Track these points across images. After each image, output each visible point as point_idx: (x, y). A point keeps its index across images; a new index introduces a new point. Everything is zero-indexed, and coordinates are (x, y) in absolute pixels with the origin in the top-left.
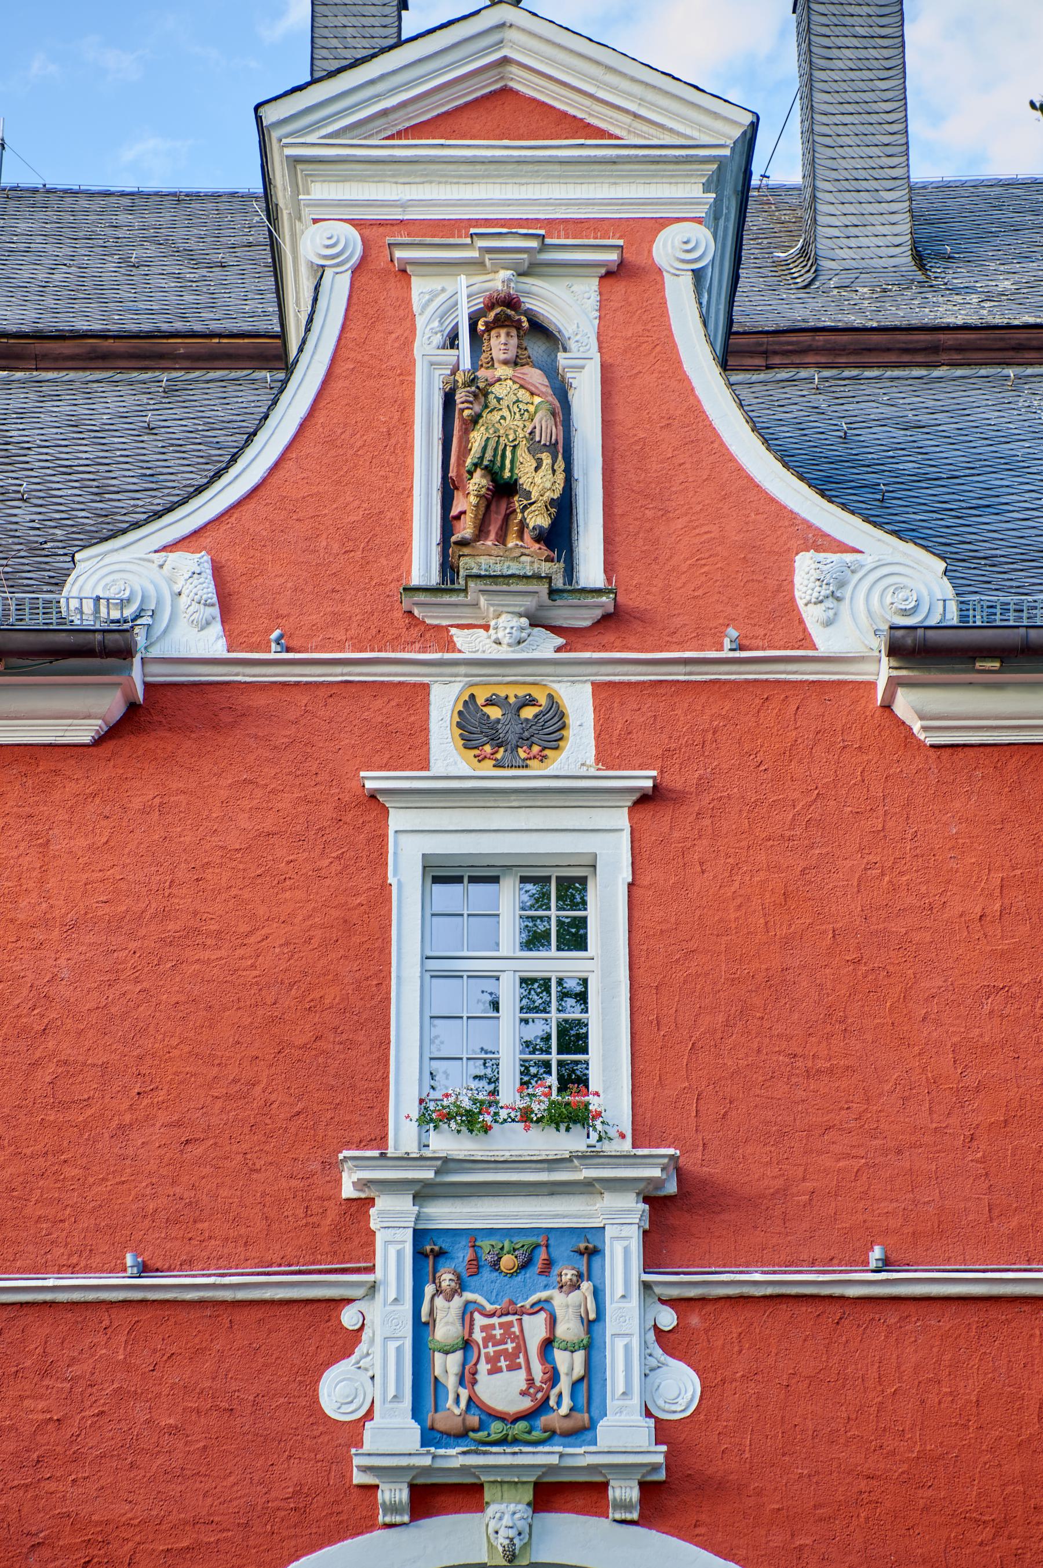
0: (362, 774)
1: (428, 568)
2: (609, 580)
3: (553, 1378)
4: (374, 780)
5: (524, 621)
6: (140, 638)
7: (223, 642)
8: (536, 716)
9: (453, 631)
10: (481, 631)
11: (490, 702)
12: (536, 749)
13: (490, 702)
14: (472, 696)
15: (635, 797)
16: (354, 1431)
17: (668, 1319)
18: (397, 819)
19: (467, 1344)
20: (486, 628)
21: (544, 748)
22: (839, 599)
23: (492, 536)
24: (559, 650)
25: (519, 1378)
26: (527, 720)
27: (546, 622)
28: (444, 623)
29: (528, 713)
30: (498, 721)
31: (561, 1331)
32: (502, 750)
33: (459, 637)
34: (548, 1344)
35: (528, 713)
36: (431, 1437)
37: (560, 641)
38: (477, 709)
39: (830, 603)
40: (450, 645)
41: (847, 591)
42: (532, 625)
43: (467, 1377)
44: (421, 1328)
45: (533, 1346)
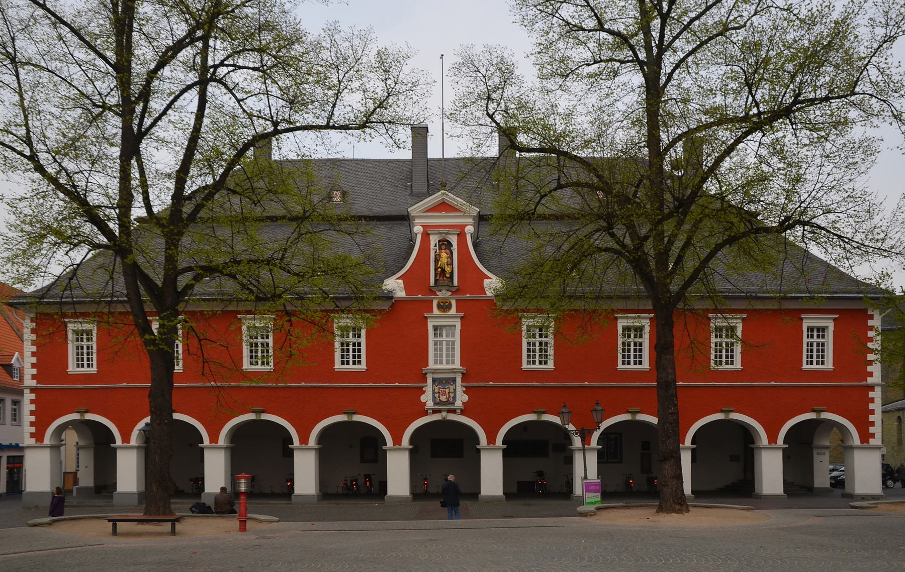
3: (450, 397)
4: (426, 315)
16: (425, 403)
17: (464, 389)
18: (429, 320)
19: (439, 392)
24: (451, 295)
25: (445, 397)
29: (447, 304)
31: (451, 391)
33: (438, 293)
34: (449, 393)
35: (447, 304)
36: (435, 404)
43: (439, 397)
44: (433, 390)
45: (447, 393)
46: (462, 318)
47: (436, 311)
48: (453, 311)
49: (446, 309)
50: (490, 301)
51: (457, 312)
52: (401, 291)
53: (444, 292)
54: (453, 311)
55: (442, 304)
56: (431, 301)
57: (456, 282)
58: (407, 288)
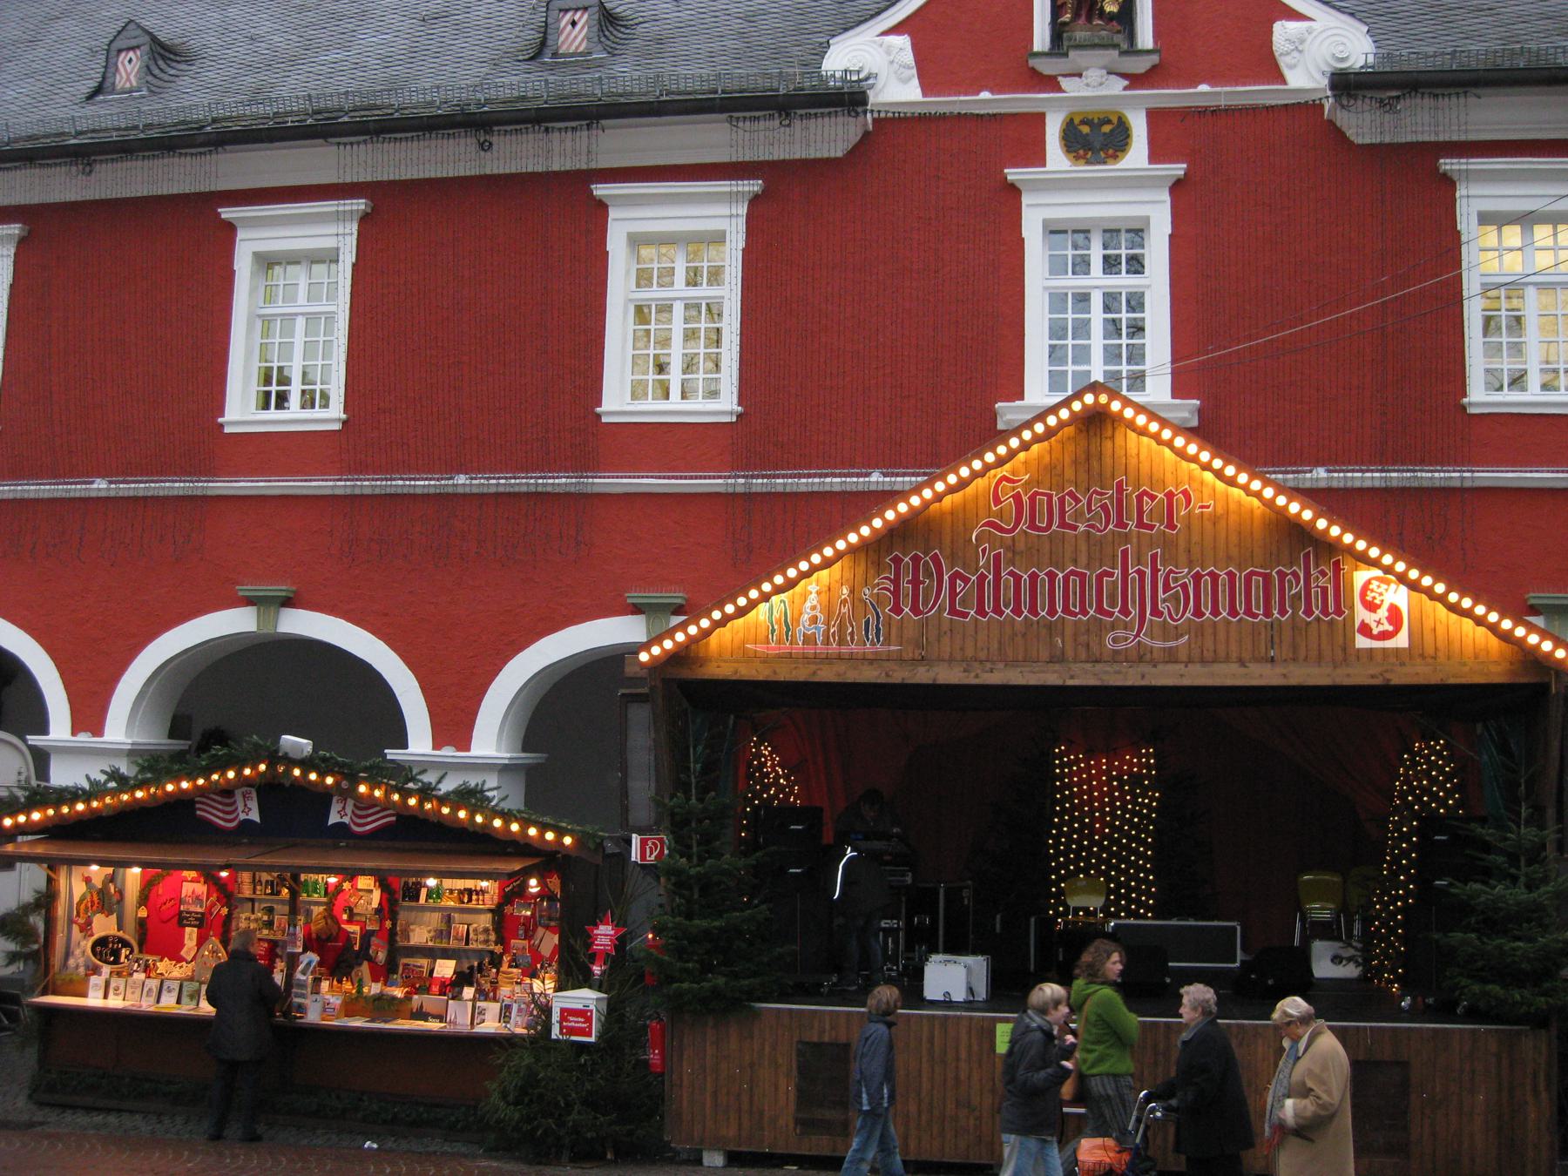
0: (1006, 171)
1: (1043, 40)
2: (1155, 42)
5: (1104, 72)
6: (871, 93)
7: (919, 90)
8: (1111, 131)
9: (1060, 79)
10: (1077, 79)
11: (1083, 122)
12: (1111, 151)
13: (1083, 122)
14: (1072, 120)
15: (1175, 179)
20: (1080, 75)
21: (1116, 151)
22: (1300, 52)
23: (1083, 18)
24: (1125, 88)
26: (1105, 134)
27: (1118, 71)
28: (1054, 73)
29: (1106, 129)
30: (1087, 135)
32: (1090, 153)
35: (1106, 129)
37: (1126, 83)
38: (1075, 128)
39: (1295, 54)
40: (1059, 89)
41: (1305, 46)
42: (1109, 73)
46: (1177, 187)
47: (1056, 157)
48: (1137, 154)
49: (1104, 147)
50: (1307, 109)
51: (1154, 156)
52: (906, 81)
53: (1093, 75)
54: (1137, 154)
55: (1085, 129)
56: (1039, 119)
57: (1145, 35)
58: (930, 72)
